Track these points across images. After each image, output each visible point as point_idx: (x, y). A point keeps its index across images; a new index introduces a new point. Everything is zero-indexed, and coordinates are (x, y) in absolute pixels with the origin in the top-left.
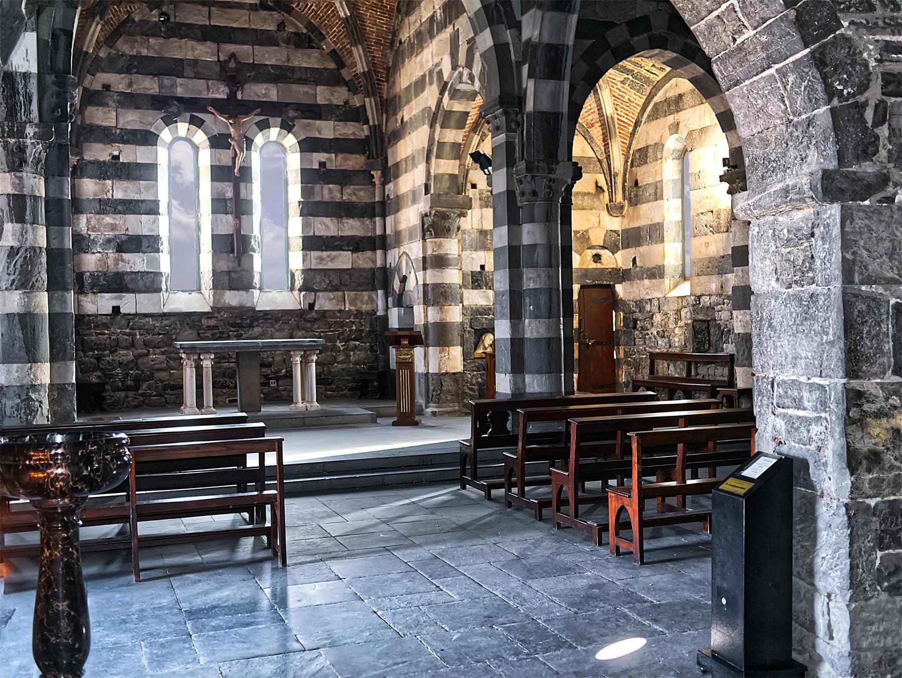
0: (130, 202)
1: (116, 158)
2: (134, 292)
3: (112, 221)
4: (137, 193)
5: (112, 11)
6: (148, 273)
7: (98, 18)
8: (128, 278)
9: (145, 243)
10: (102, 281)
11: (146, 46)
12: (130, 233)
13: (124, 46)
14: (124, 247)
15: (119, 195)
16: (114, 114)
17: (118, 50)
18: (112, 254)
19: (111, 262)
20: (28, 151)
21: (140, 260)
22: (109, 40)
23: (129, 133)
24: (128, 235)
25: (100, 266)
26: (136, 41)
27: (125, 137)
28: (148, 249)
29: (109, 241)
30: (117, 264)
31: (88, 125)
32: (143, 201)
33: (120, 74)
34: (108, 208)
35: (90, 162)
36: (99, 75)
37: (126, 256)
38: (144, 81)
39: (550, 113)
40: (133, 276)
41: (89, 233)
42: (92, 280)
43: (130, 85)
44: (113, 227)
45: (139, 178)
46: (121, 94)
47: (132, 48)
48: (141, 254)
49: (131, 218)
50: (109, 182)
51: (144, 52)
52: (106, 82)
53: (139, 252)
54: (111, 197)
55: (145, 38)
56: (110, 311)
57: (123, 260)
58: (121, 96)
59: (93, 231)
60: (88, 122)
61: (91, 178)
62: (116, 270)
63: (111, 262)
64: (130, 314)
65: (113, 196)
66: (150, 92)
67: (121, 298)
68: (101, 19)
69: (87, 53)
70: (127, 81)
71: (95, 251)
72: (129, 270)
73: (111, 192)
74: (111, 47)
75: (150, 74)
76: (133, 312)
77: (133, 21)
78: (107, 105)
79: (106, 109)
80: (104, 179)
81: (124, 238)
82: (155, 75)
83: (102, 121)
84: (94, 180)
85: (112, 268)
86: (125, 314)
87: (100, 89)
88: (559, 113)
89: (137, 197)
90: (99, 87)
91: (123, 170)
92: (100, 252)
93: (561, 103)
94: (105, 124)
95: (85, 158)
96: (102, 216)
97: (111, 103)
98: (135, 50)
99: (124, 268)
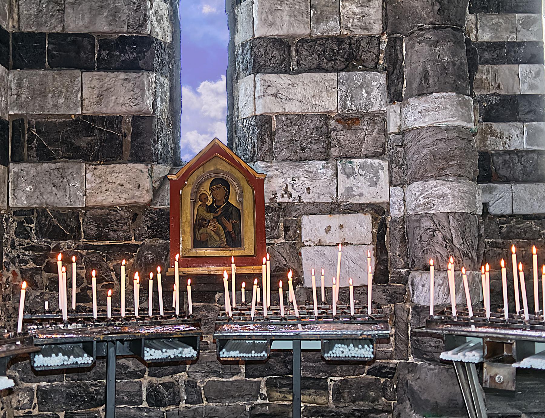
0: (500, 45)
2: (507, 181)
4: (511, 32)
6: (528, 152)
9: (523, 107)
12: (503, 93)
21: (518, 132)
24: (499, 95)
28: (529, 116)
32: (520, 44)
37: (497, 127)
40: (507, 157)
49: (504, 69)
57: (492, 134)
64: (503, 216)
65: (476, 37)
67: (490, 191)
72: (501, 148)
73: (474, 32)
76: (508, 212)
81: (494, 100)
89: (512, 38)
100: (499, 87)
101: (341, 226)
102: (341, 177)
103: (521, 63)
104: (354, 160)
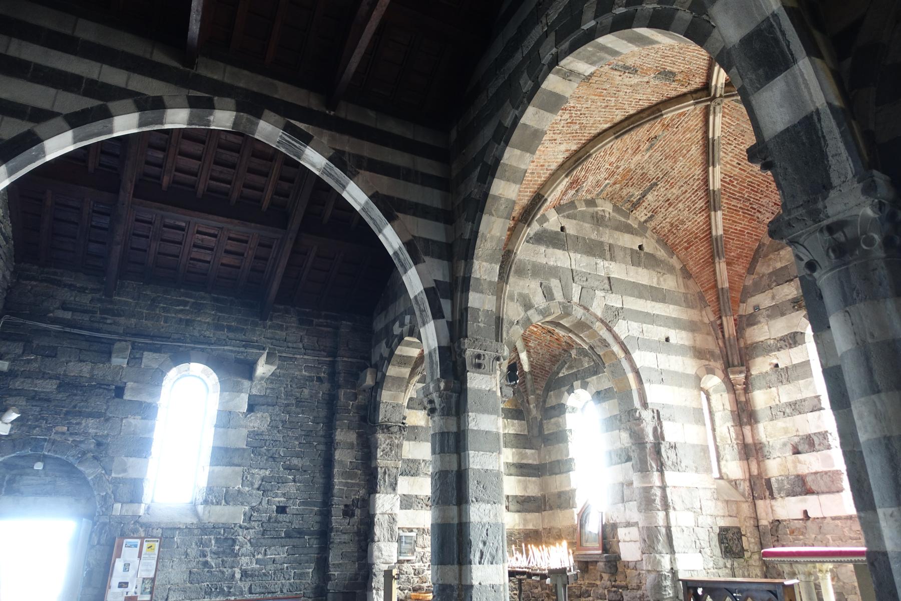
0: (795, 403)
1: (777, 366)
2: (818, 493)
3: (784, 425)
5: (737, 247)
7: (717, 260)
8: (809, 479)
9: (817, 442)
10: (787, 486)
11: (778, 259)
12: (801, 434)
13: (763, 269)
14: (800, 448)
15: (785, 399)
16: (766, 327)
17: (758, 274)
18: (791, 458)
19: (790, 465)
20: (436, 401)
22: (751, 270)
23: (781, 340)
24: (799, 436)
25: (783, 470)
26: (771, 259)
27: (779, 345)
28: (821, 448)
29: (785, 445)
30: (795, 467)
31: (750, 344)
32: (805, 400)
33: (764, 292)
34: (779, 413)
35: (757, 376)
36: (749, 300)
38: (783, 290)
39: (795, 126)
40: (813, 477)
41: (768, 440)
42: (778, 484)
43: (773, 298)
44: (786, 430)
45: (798, 378)
46: (767, 309)
47: (769, 266)
48: (814, 453)
49: (798, 418)
50: (774, 389)
51: (779, 265)
52: (755, 304)
53: (813, 451)
54: (778, 403)
55: (776, 253)
56: (801, 516)
57: (800, 462)
58: (768, 310)
59: (771, 437)
60: (749, 342)
61: (760, 389)
62: (795, 473)
63: (790, 465)
64: (818, 518)
66: (790, 297)
68: (720, 259)
69: (722, 288)
70: (770, 295)
71: (776, 457)
73: (777, 397)
74: (753, 274)
75: (786, 282)
77: (764, 244)
78: (759, 322)
79: (760, 326)
80: (770, 388)
81: (796, 439)
82: (792, 280)
83: (760, 337)
84: (762, 391)
85: (793, 472)
86: (814, 518)
87: (753, 311)
88: (812, 115)
89: (799, 397)
90: (750, 310)
91: (783, 375)
92: (779, 457)
93: (808, 98)
94: (762, 339)
95: (753, 373)
96: (775, 422)
97: (762, 320)
98: (771, 267)
99: (803, 470)
100: (797, 431)
101: (629, 533)
102: (627, 510)
103: (808, 412)
104: (630, 502)
